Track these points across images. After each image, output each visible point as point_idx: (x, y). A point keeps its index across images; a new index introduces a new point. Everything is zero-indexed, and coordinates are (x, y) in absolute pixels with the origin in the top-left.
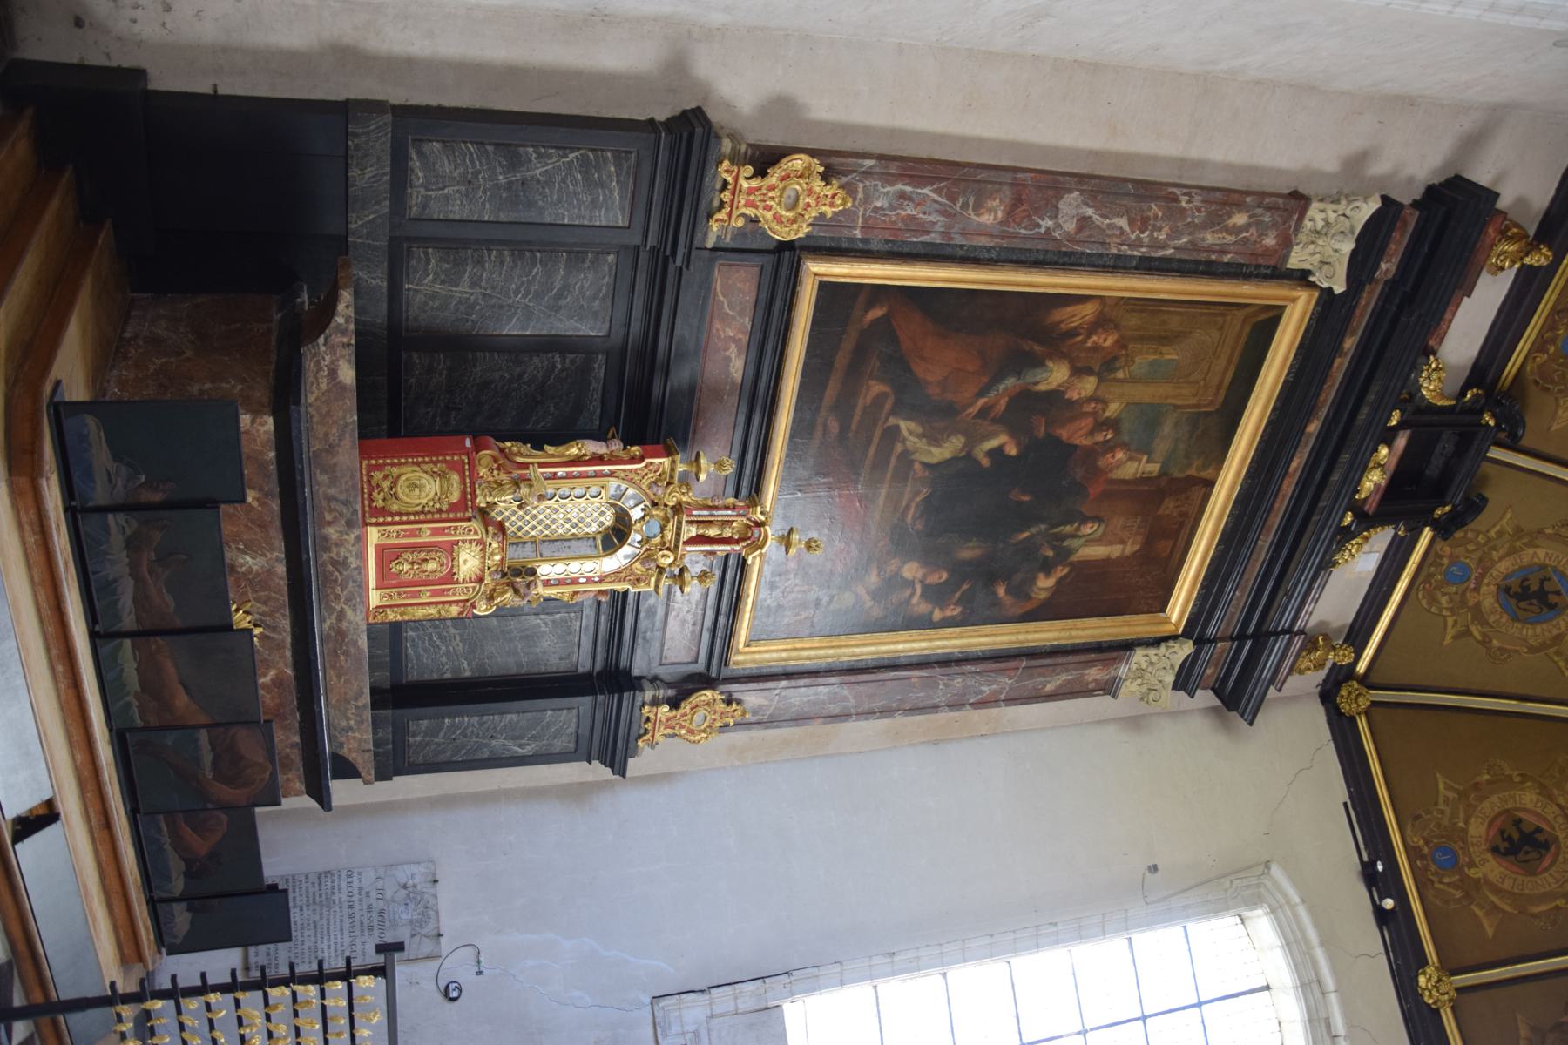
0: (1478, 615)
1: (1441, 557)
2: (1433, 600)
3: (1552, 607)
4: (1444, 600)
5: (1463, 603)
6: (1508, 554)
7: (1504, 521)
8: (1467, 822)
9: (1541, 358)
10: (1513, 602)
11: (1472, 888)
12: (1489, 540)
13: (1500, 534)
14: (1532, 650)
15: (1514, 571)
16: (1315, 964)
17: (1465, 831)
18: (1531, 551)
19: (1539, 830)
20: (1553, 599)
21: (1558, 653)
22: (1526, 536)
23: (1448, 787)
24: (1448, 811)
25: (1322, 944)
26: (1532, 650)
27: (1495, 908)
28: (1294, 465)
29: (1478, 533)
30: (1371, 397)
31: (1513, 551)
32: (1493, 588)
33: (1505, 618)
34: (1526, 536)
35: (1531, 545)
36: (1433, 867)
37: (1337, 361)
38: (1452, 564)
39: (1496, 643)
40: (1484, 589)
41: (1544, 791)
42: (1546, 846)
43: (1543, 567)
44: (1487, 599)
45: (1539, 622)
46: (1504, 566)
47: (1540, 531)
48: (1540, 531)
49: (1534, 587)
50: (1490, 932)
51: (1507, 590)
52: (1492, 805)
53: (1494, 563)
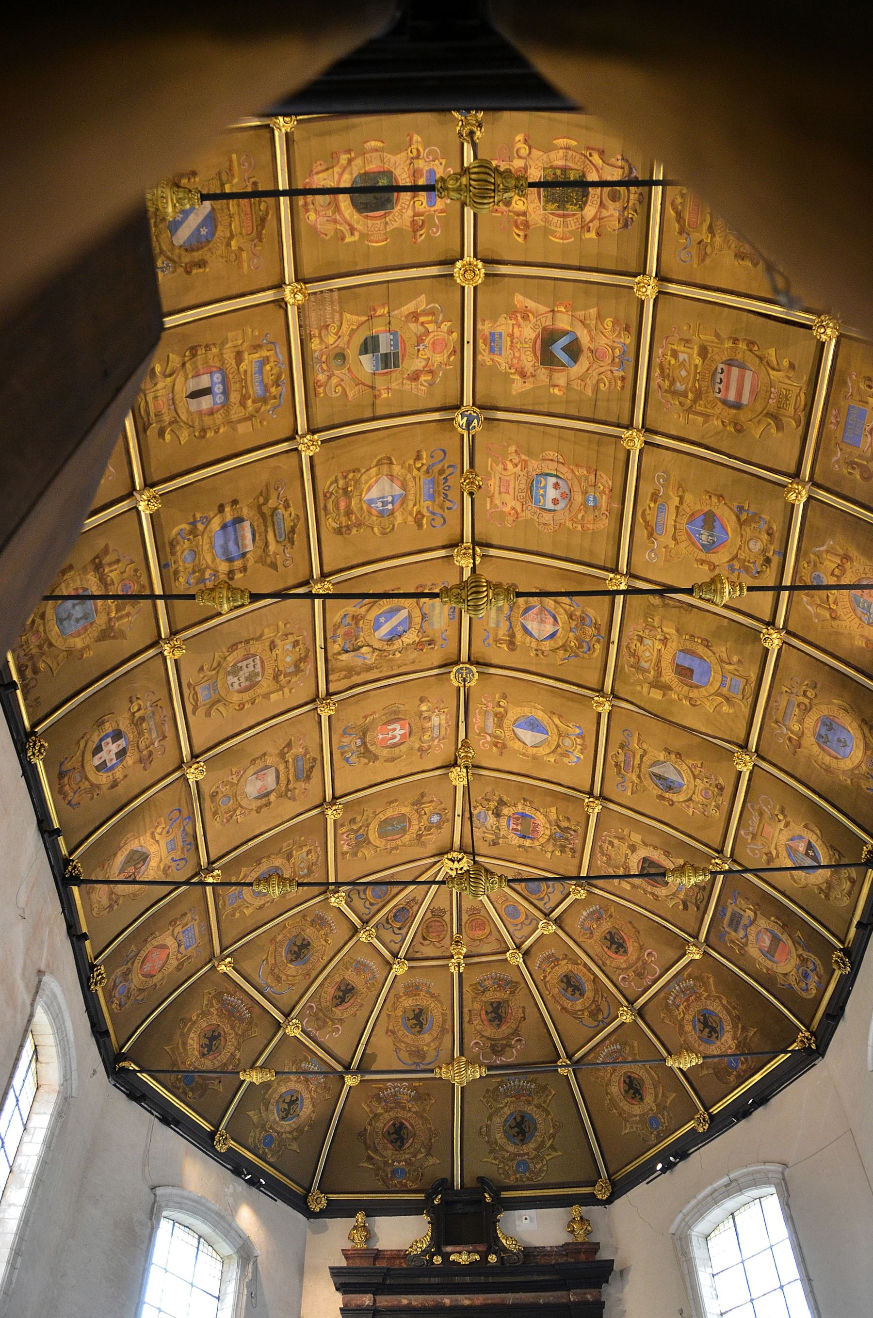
0: (541, 1145)
1: (517, 1179)
2: (541, 1171)
3: (523, 1117)
4: (538, 1166)
5: (536, 1157)
6: (504, 1149)
7: (489, 1160)
8: (635, 1116)
9: (409, 1184)
10: (527, 1135)
11: (661, 1107)
12: (500, 1162)
13: (495, 1158)
14: (548, 1113)
15: (512, 1142)
16: (705, 1198)
17: (640, 1115)
18: (499, 1141)
19: (625, 1082)
20: (519, 1119)
21: (545, 1102)
22: (493, 1147)
23: (626, 1128)
24: (635, 1126)
25: (695, 1197)
26: (548, 1113)
27: (663, 1094)
28: (467, 1302)
29: (499, 1168)
30: (426, 1280)
31: (502, 1148)
32: (524, 1147)
33: (537, 1134)
34: (493, 1147)
35: (496, 1143)
36: (661, 1128)
37: (414, 1303)
38: (520, 1172)
39: (551, 1131)
40: (526, 1151)
41: (609, 1083)
42: (630, 1077)
43: (505, 1132)
44: (530, 1147)
45: (533, 1118)
46: (511, 1148)
47: (488, 1142)
48: (488, 1142)
49: (516, 1130)
50: (674, 1095)
51: (522, 1140)
52: (624, 1105)
53: (511, 1153)
